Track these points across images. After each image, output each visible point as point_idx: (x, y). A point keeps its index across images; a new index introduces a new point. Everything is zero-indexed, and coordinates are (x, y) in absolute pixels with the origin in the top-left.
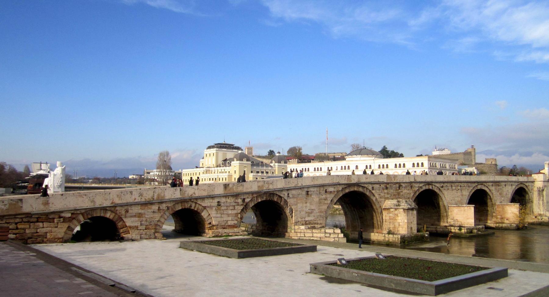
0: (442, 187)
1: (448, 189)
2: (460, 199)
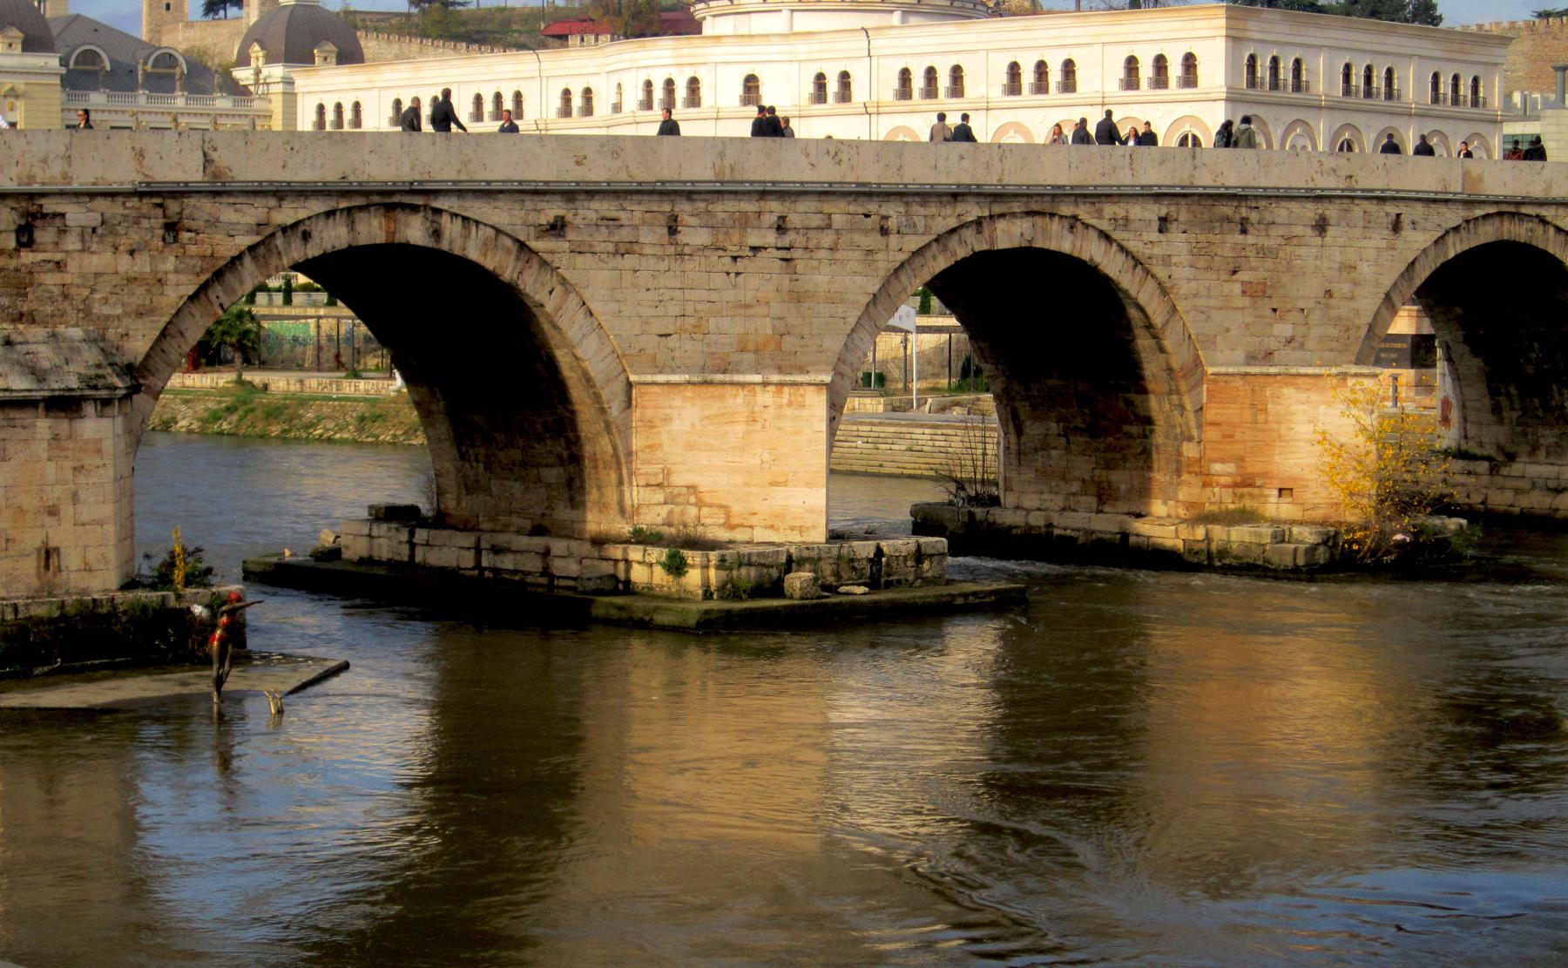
0: (557, 228)
1: (625, 249)
2: (765, 327)
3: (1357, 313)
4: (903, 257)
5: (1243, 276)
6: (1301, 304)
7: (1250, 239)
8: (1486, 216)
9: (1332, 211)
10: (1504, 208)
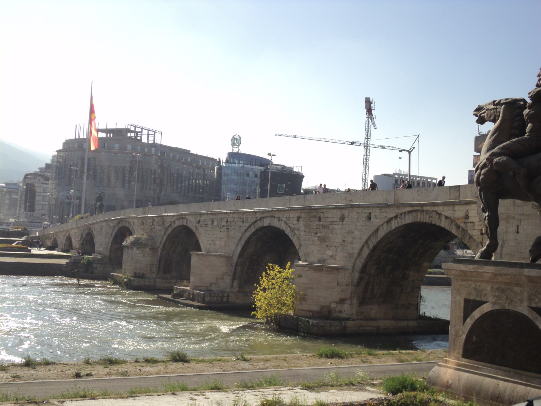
3: (353, 248)
4: (246, 228)
5: (318, 235)
6: (335, 244)
7: (321, 223)
8: (409, 212)
9: (346, 212)
10: (416, 208)
